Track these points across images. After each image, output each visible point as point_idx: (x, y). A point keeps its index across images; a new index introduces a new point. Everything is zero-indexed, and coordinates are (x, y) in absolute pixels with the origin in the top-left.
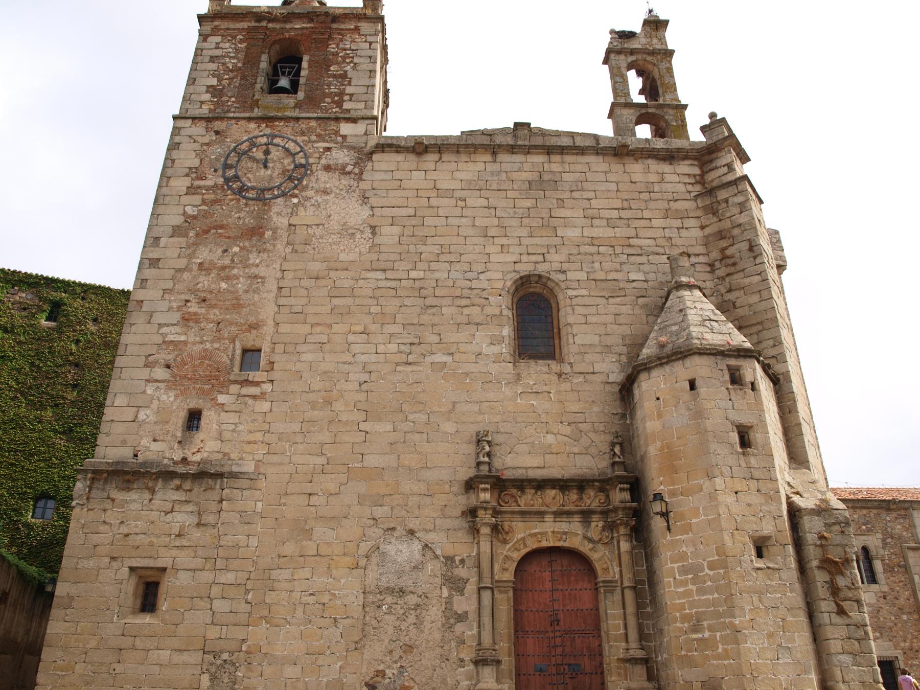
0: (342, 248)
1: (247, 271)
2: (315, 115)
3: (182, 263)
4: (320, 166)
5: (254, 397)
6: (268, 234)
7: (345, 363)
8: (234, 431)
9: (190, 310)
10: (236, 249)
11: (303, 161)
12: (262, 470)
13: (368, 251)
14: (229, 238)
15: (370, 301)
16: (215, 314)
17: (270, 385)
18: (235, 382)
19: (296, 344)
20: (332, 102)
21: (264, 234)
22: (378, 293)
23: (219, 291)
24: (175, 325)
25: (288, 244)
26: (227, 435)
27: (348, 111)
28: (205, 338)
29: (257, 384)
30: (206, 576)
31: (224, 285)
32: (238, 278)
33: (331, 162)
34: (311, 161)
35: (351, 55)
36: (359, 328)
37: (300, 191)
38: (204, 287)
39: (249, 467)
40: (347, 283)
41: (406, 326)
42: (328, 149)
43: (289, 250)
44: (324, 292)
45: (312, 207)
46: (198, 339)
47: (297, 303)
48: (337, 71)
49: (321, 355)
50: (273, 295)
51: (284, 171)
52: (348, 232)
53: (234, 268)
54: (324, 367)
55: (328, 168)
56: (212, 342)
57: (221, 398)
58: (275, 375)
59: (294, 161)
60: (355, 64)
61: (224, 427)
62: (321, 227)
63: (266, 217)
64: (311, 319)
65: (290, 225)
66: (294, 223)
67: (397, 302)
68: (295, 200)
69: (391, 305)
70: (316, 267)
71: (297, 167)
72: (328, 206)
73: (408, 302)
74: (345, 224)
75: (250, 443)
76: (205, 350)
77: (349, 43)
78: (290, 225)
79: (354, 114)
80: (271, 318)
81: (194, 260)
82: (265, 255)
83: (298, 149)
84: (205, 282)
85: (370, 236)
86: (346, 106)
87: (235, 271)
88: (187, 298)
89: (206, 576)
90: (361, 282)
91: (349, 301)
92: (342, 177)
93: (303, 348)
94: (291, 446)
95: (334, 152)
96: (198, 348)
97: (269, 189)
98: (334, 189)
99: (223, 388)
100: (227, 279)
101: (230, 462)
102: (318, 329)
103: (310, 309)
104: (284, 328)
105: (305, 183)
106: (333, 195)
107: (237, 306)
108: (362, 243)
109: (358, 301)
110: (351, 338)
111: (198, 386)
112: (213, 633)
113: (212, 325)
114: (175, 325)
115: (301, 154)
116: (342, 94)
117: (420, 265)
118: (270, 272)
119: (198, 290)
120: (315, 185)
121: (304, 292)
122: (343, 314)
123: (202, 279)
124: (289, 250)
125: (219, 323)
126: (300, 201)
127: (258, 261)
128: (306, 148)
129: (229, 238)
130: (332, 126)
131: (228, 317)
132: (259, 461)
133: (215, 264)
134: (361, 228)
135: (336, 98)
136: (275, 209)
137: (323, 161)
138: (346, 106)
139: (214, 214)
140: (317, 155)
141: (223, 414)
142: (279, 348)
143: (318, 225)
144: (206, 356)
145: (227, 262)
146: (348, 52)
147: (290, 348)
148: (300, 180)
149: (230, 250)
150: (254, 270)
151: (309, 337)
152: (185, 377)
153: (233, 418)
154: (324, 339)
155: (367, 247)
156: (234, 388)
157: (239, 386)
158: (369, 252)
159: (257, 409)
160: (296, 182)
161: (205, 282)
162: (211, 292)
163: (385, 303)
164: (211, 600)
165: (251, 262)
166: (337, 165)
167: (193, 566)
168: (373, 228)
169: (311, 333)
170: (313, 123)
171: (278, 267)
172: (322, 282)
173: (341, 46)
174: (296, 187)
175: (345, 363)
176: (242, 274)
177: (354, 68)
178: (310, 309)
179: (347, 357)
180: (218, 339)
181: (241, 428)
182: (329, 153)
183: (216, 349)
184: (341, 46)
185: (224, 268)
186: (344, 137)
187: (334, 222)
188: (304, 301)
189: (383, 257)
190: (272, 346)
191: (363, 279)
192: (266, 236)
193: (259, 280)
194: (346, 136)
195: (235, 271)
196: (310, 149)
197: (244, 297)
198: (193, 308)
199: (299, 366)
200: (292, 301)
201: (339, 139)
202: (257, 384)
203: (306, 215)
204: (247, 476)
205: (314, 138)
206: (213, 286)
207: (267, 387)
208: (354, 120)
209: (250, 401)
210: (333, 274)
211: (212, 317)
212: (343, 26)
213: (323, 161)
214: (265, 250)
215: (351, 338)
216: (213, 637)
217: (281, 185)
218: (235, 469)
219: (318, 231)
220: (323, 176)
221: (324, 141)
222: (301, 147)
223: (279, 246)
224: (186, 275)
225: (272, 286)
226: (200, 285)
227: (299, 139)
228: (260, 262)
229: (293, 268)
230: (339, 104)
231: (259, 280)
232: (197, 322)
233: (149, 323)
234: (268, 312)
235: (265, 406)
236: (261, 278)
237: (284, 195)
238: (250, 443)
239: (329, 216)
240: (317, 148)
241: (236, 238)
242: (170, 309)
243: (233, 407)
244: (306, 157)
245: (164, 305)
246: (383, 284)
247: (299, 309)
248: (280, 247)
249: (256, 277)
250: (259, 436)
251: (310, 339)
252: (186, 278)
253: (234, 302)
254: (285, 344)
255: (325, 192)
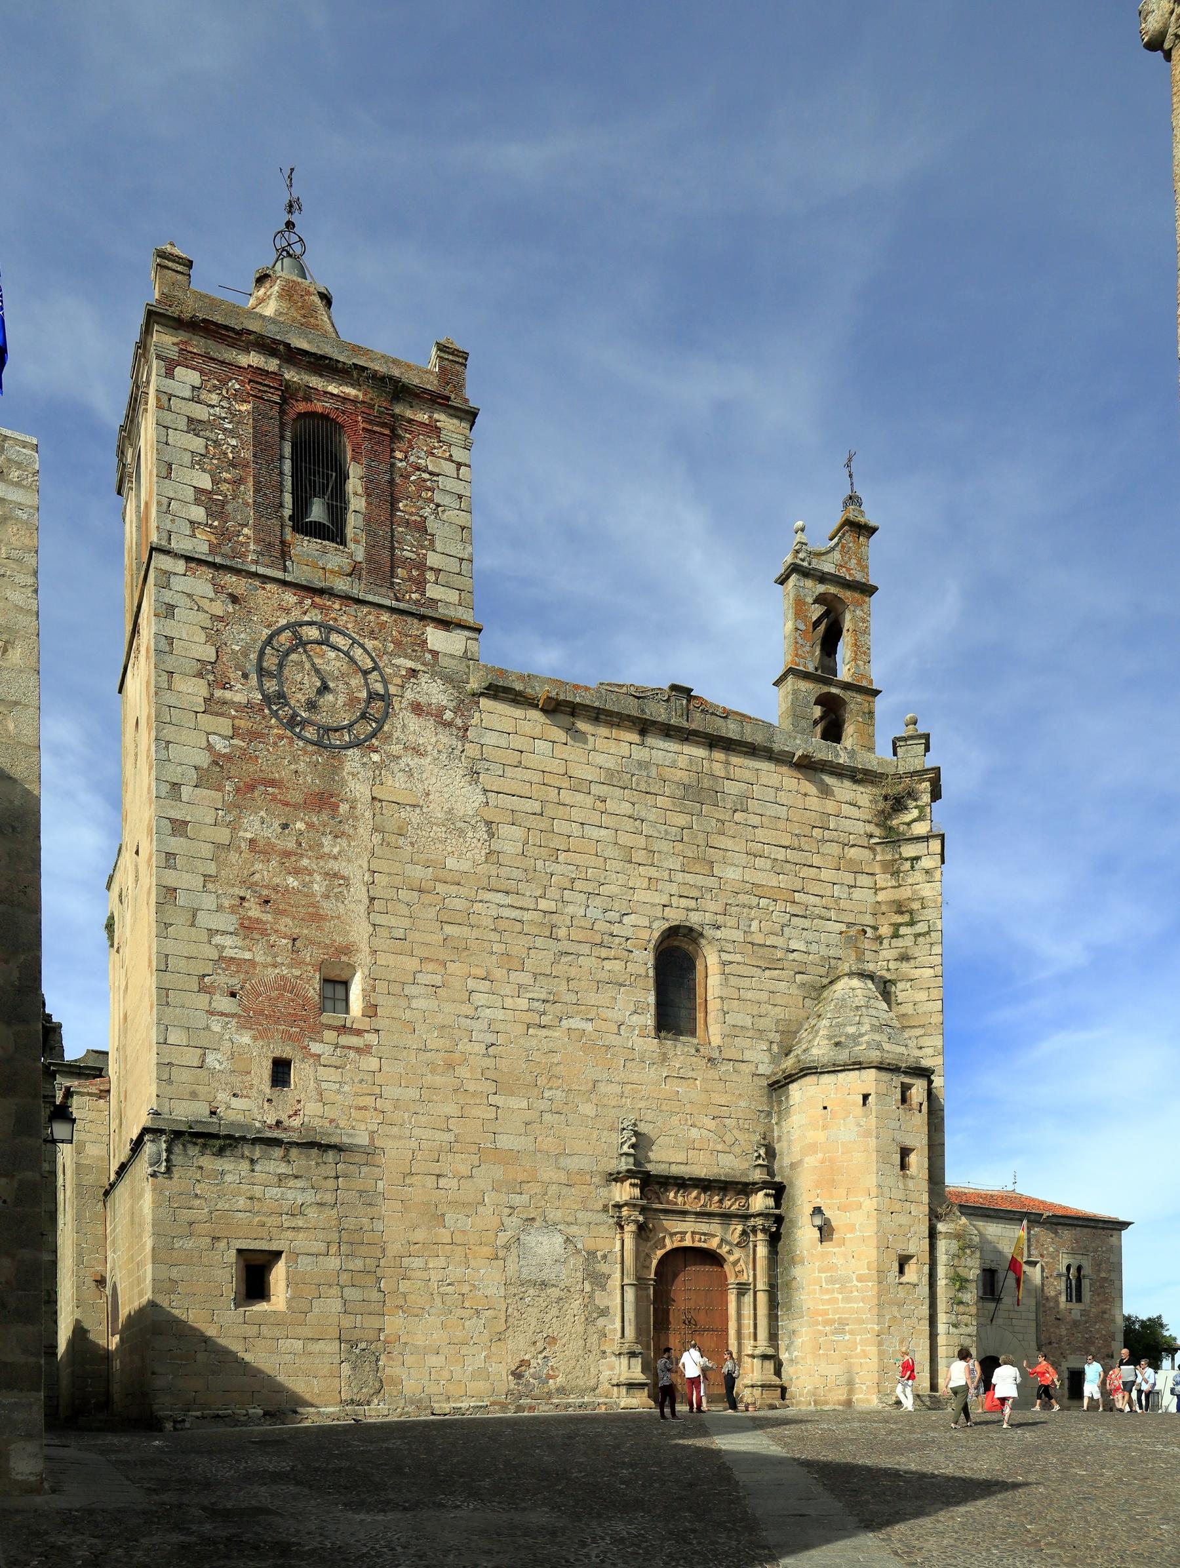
0: (449, 849)
1: (322, 863)
2: (387, 602)
3: (223, 835)
4: (405, 704)
5: (358, 1050)
6: (344, 808)
7: (467, 1017)
8: (338, 1092)
9: (250, 914)
10: (300, 825)
11: (379, 688)
12: (377, 1143)
13: (483, 859)
14: (287, 804)
15: (494, 936)
16: (286, 924)
17: (376, 1035)
18: (330, 1027)
19: (404, 983)
20: (410, 579)
21: (338, 806)
22: (503, 924)
23: (287, 890)
24: (231, 933)
25: (375, 829)
26: (329, 1096)
27: (434, 602)
28: (279, 960)
29: (359, 1033)
30: (333, 1263)
31: (292, 882)
32: (310, 874)
33: (422, 700)
34: (392, 690)
35: (428, 483)
36: (482, 973)
37: (384, 744)
38: (263, 880)
39: (363, 1139)
40: (459, 904)
41: (539, 978)
42: (413, 673)
43: (377, 838)
44: (432, 913)
45: (401, 774)
46: (269, 959)
47: (399, 923)
48: (411, 514)
49: (437, 1002)
50: (362, 909)
51: (352, 701)
52: (453, 824)
53: (302, 856)
54: (440, 1019)
55: (417, 709)
56: (290, 966)
57: (315, 1048)
58: (380, 1023)
59: (367, 684)
60: (438, 506)
61: (324, 1085)
62: (418, 810)
63: (337, 778)
64: (420, 951)
65: (373, 798)
66: (379, 796)
67: (524, 941)
68: (376, 757)
69: (518, 946)
70: (418, 873)
71: (372, 696)
72: (424, 776)
73: (539, 942)
74: (451, 810)
75: (360, 1108)
76: (283, 977)
77: (422, 454)
78: (373, 798)
79: (442, 611)
80: (365, 941)
81: (241, 834)
82: (343, 842)
83: (370, 665)
84: (266, 872)
85: (486, 836)
86: (432, 591)
87: (305, 862)
88: (242, 894)
89: (333, 1263)
90: (478, 907)
91: (466, 930)
92: (440, 730)
93: (410, 990)
94: (410, 1118)
95: (424, 679)
96: (272, 973)
97: (336, 730)
98: (430, 748)
99: (316, 1032)
100: (296, 872)
101: (339, 1131)
102: (430, 967)
103: (414, 936)
104: (382, 959)
105: (386, 728)
106: (429, 759)
107: (316, 917)
108: (475, 844)
109: (476, 933)
110: (471, 984)
111: (281, 1028)
112: (347, 1322)
113: (284, 941)
114: (231, 933)
115: (375, 673)
116: (421, 566)
117: (553, 893)
118: (355, 870)
119: (256, 884)
120: (402, 736)
121: (404, 910)
122: (461, 949)
123: (258, 866)
124: (377, 838)
125: (294, 940)
126: (383, 761)
127: (336, 850)
128: (381, 665)
129: (287, 804)
130: (414, 626)
131: (306, 931)
132: (374, 1132)
133: (274, 845)
134: (473, 822)
135: (415, 573)
136: (348, 767)
137: (409, 695)
138: (432, 591)
139: (257, 757)
140: (398, 681)
141: (321, 1068)
142: (381, 986)
143: (414, 806)
144: (284, 985)
145: (291, 845)
146: (426, 476)
147: (396, 988)
148: (381, 723)
149: (291, 826)
150: (333, 865)
151: (418, 976)
152: (262, 1013)
153: (334, 1074)
154: (438, 980)
155: (483, 854)
156: (330, 1035)
157: (336, 1034)
158: (486, 862)
159: (363, 1066)
160: (374, 725)
161: (266, 872)
162: (275, 889)
163: (509, 941)
164: (342, 1287)
165: (326, 850)
166: (430, 705)
167: (314, 1250)
168: (489, 823)
169: (421, 971)
170: (385, 617)
171: (365, 867)
172: (427, 898)
173: (412, 459)
174: (374, 735)
175: (467, 1017)
176: (315, 867)
177: (435, 512)
178: (414, 936)
179: (467, 1009)
180: (299, 963)
181: (346, 1088)
182: (415, 681)
183: (297, 977)
184: (412, 459)
185: (287, 854)
186: (435, 654)
187: (435, 806)
188: (406, 923)
189: (504, 872)
190: (372, 982)
191: (481, 901)
192: (341, 810)
193: (341, 882)
194: (438, 653)
195: (305, 862)
196: (386, 666)
197: (325, 904)
198: (254, 911)
199: (408, 1015)
200: (393, 921)
201: (428, 656)
202: (359, 1033)
203: (396, 784)
204: (362, 1150)
205: (391, 646)
206: (277, 880)
207: (371, 1038)
208: (446, 624)
209: (352, 1054)
210: (440, 887)
211: (283, 928)
212: (409, 414)
213: (409, 695)
214: (343, 833)
215: (471, 984)
216: (348, 1326)
217: (351, 725)
218: (345, 1140)
219: (415, 817)
220: (413, 722)
221: (405, 657)
222: (373, 659)
223: (361, 831)
224: (233, 857)
225: (359, 892)
226: (257, 877)
227: (369, 644)
228: (339, 853)
229: (386, 870)
230: (421, 584)
231: (341, 882)
232: (264, 933)
233: (193, 925)
234: (359, 932)
235: (373, 1063)
236: (343, 878)
237: (356, 744)
238: (360, 1108)
239: (428, 794)
240: (398, 667)
241: (296, 807)
242: (220, 908)
243: (334, 1061)
244: (385, 682)
245: (209, 901)
246: (506, 912)
247: (400, 933)
248: (363, 831)
249: (335, 875)
250: (368, 1101)
251: (421, 978)
252: (234, 861)
253: (310, 910)
254: (389, 981)
255: (417, 751)
